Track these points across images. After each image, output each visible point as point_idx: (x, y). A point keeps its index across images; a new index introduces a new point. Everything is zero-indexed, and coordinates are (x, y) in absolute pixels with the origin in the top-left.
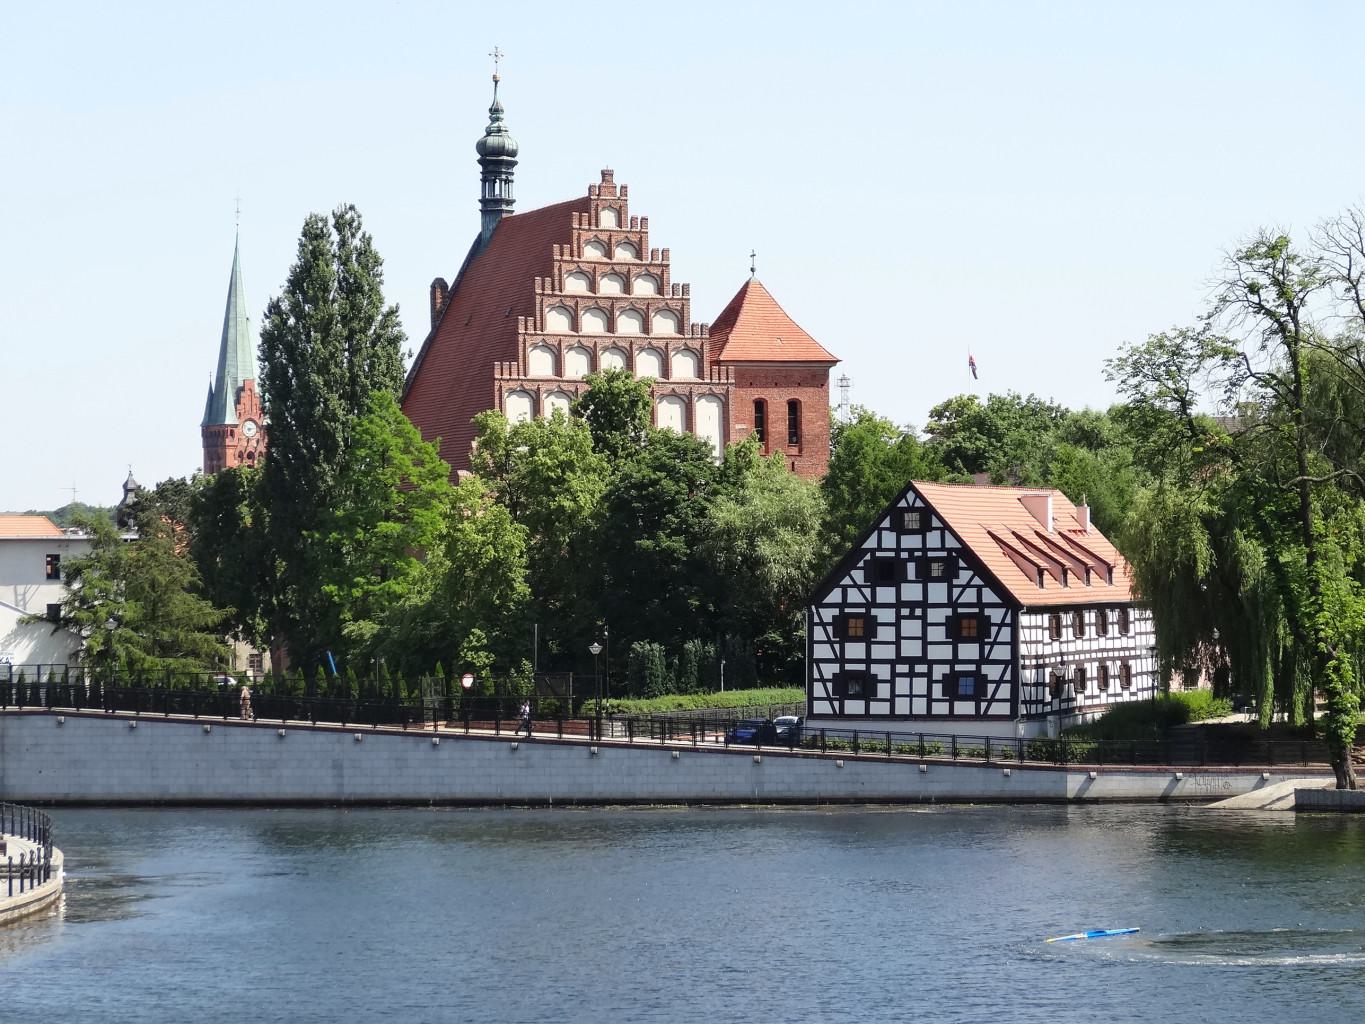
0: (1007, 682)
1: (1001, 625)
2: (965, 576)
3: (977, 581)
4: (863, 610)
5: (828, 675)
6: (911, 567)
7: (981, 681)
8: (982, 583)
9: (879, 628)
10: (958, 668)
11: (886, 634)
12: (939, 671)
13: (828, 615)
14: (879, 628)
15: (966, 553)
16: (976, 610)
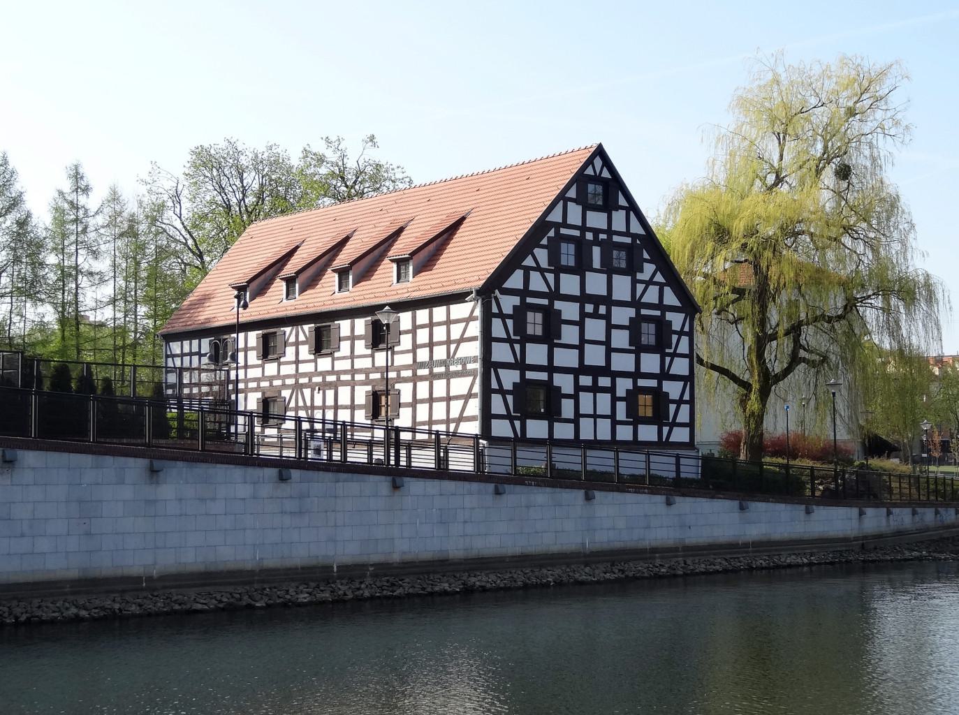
0: (686, 402)
1: (681, 333)
2: (649, 268)
3: (659, 278)
4: (545, 302)
5: (508, 386)
6: (596, 251)
7: (660, 398)
8: (662, 280)
9: (564, 327)
10: (642, 383)
11: (569, 334)
12: (624, 385)
13: (509, 303)
14: (564, 327)
15: (650, 240)
16: (658, 313)
